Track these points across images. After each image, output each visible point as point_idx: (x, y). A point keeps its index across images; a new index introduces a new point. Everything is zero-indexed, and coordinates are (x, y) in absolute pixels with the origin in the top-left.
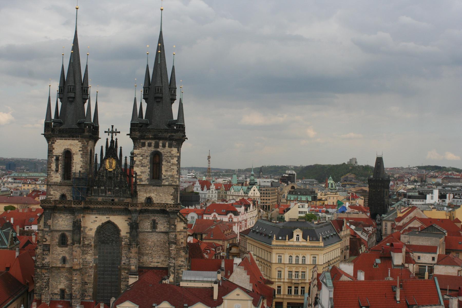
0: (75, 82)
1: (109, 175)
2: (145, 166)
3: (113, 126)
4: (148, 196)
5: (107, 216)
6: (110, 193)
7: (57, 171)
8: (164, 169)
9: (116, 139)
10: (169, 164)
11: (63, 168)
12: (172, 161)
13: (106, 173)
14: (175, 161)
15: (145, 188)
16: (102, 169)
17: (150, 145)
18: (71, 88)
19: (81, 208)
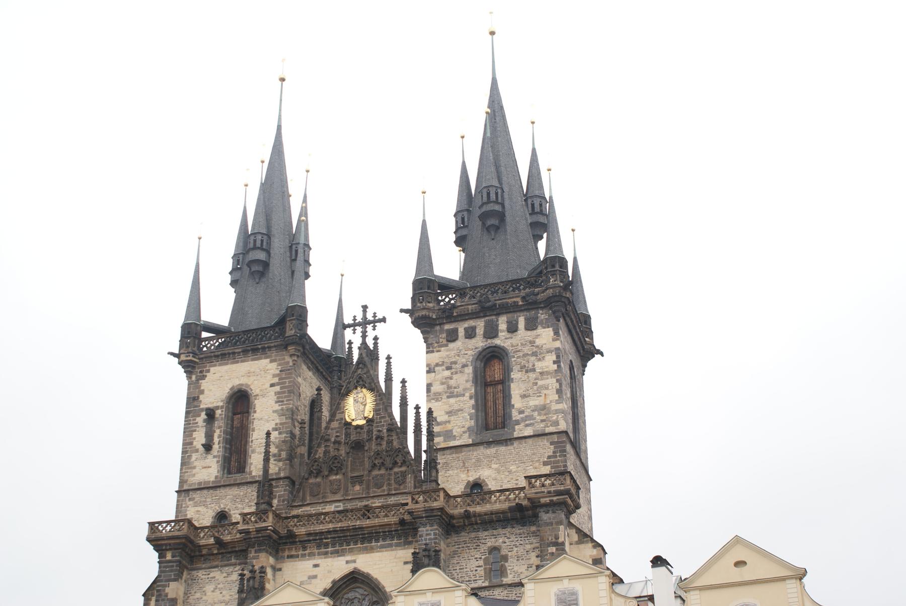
0: (269, 227)
1: (353, 437)
2: (457, 396)
3: (365, 308)
4: (471, 479)
5: (349, 558)
6: (357, 488)
7: (208, 447)
8: (516, 390)
9: (376, 338)
10: (532, 375)
11: (226, 441)
12: (539, 366)
13: (348, 435)
14: (548, 363)
15: (462, 455)
16: (335, 424)
17: (470, 334)
18: (255, 241)
19: (266, 529)
